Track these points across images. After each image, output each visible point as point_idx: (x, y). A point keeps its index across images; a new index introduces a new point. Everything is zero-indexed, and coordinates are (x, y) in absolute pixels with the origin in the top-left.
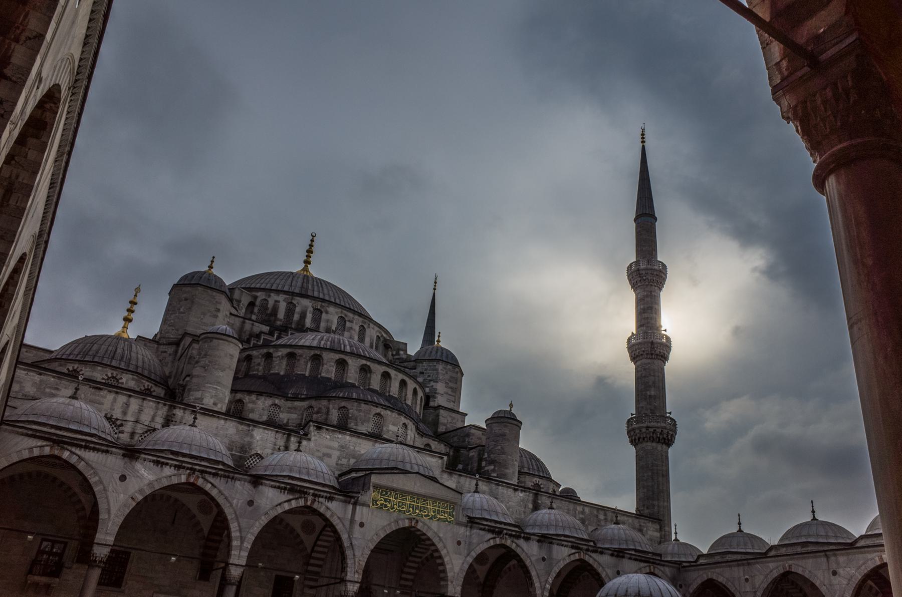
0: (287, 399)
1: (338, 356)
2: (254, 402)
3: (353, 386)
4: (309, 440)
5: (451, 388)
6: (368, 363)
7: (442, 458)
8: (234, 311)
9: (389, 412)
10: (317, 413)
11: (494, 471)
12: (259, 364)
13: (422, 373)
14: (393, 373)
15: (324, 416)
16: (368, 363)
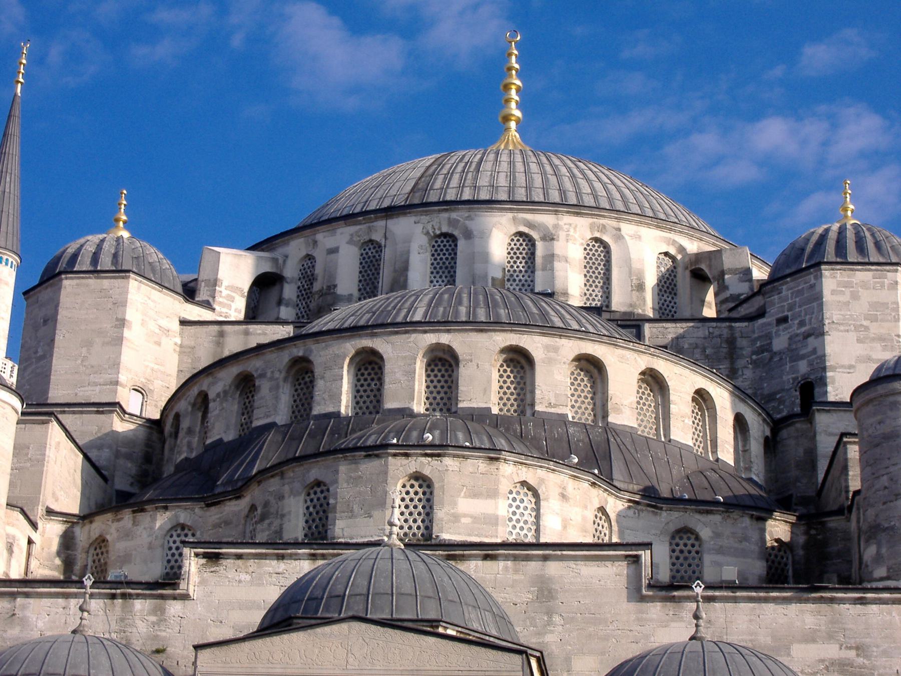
0: (212, 501)
1: (350, 347)
2: (127, 535)
3: (406, 413)
4: (185, 597)
5: (881, 339)
6: (445, 338)
7: (636, 559)
8: (194, 312)
9: (447, 461)
10: (263, 518)
11: (878, 559)
12: (190, 431)
13: (784, 320)
14: (534, 344)
15: (277, 523)
16: (445, 338)
